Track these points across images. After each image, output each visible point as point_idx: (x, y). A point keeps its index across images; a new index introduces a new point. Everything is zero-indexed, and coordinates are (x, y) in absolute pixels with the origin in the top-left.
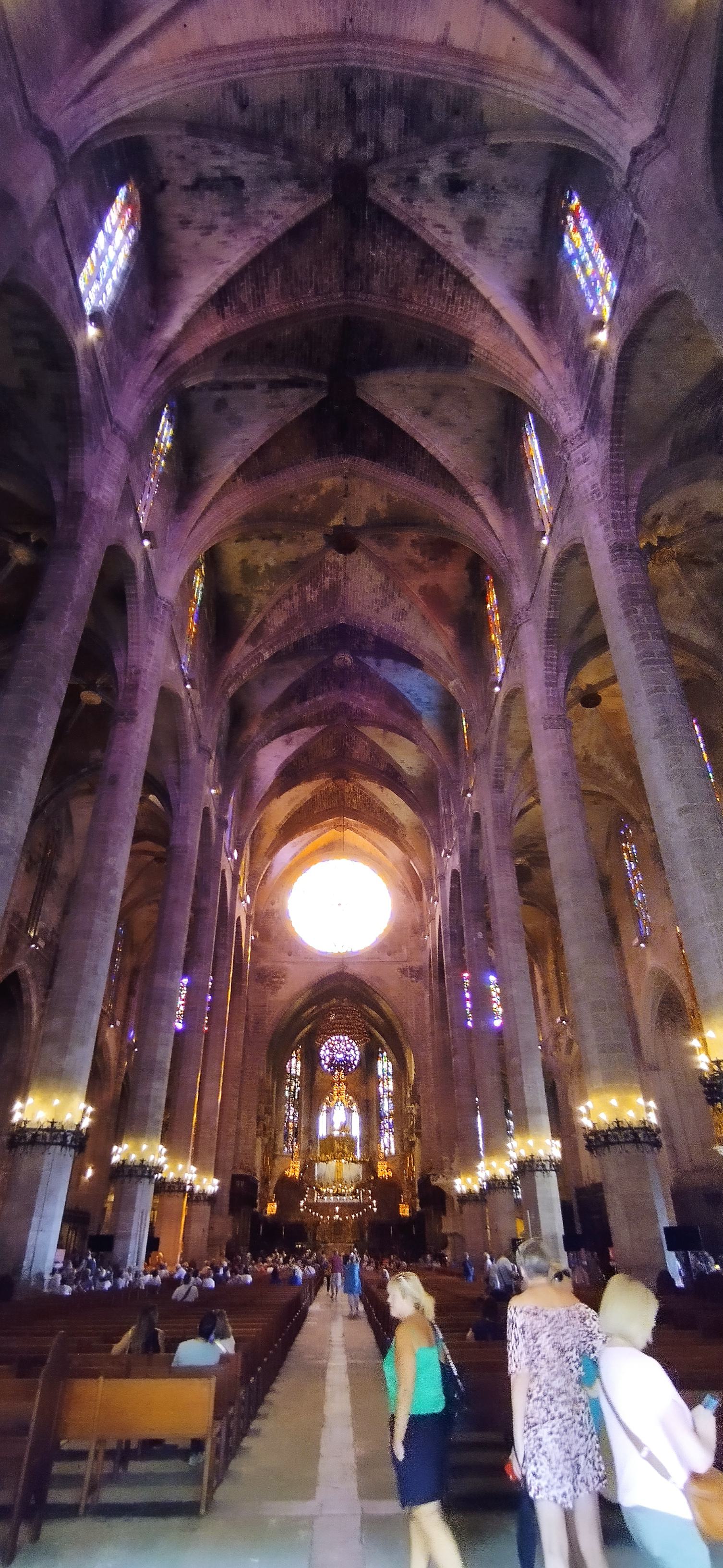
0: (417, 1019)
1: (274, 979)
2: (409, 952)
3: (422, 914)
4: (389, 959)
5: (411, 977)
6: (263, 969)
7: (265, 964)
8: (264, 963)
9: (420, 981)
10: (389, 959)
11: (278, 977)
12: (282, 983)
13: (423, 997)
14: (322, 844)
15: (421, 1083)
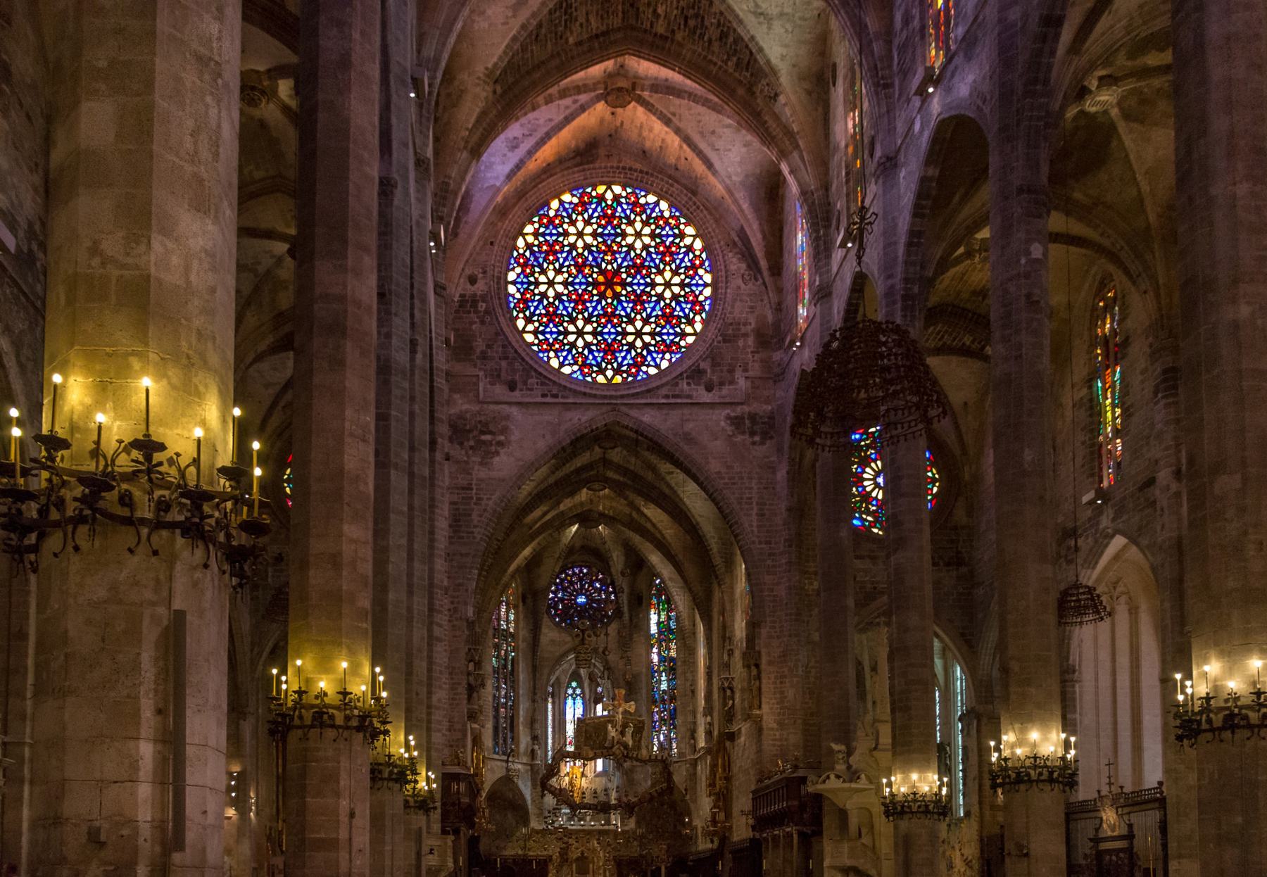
0: (761, 515)
1: (483, 437)
2: (749, 384)
3: (779, 304)
4: (706, 397)
5: (752, 434)
6: (461, 416)
7: (465, 407)
8: (462, 405)
9: (768, 441)
10: (706, 397)
11: (491, 433)
12: (500, 444)
13: (774, 473)
14: (573, 144)
15: (764, 632)
